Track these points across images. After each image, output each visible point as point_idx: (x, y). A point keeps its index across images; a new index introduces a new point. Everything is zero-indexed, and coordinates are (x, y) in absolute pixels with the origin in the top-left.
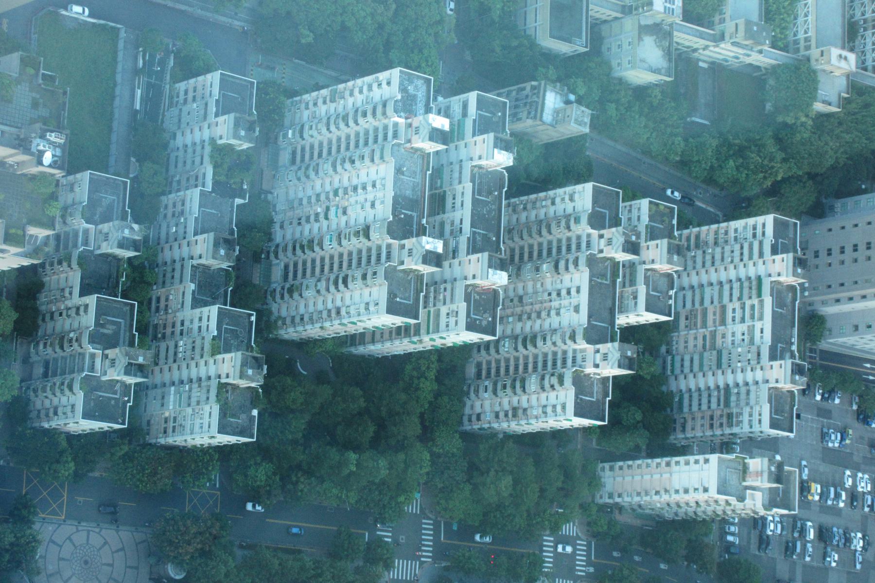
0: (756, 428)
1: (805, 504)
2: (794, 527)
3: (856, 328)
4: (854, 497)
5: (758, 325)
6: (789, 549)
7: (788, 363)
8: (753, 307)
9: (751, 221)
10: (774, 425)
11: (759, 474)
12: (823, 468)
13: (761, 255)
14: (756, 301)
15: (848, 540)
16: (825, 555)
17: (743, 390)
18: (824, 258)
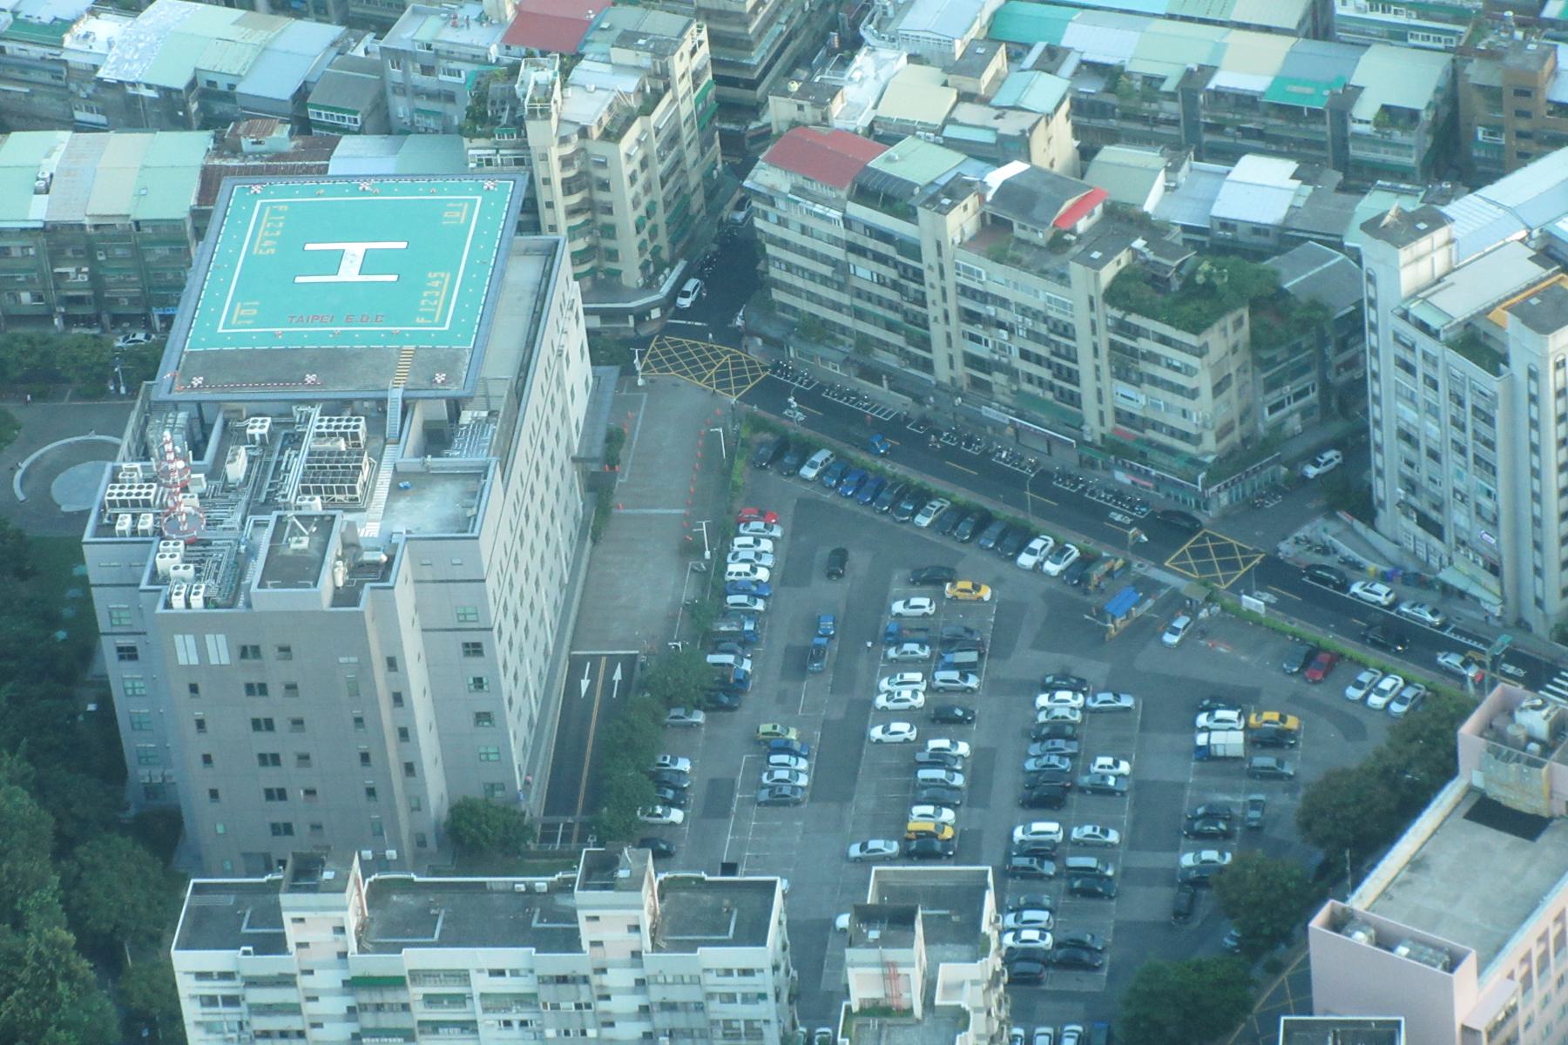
0: (765, 982)
1: (964, 847)
2: (1027, 874)
3: (483, 717)
4: (939, 717)
5: (482, 984)
6: (1090, 888)
7: (585, 900)
8: (431, 1000)
9: (191, 1012)
10: (754, 934)
11: (890, 972)
12: (865, 799)
13: (286, 981)
14: (416, 993)
15: (1058, 729)
16: (1101, 791)
17: (662, 1020)
18: (293, 809)
